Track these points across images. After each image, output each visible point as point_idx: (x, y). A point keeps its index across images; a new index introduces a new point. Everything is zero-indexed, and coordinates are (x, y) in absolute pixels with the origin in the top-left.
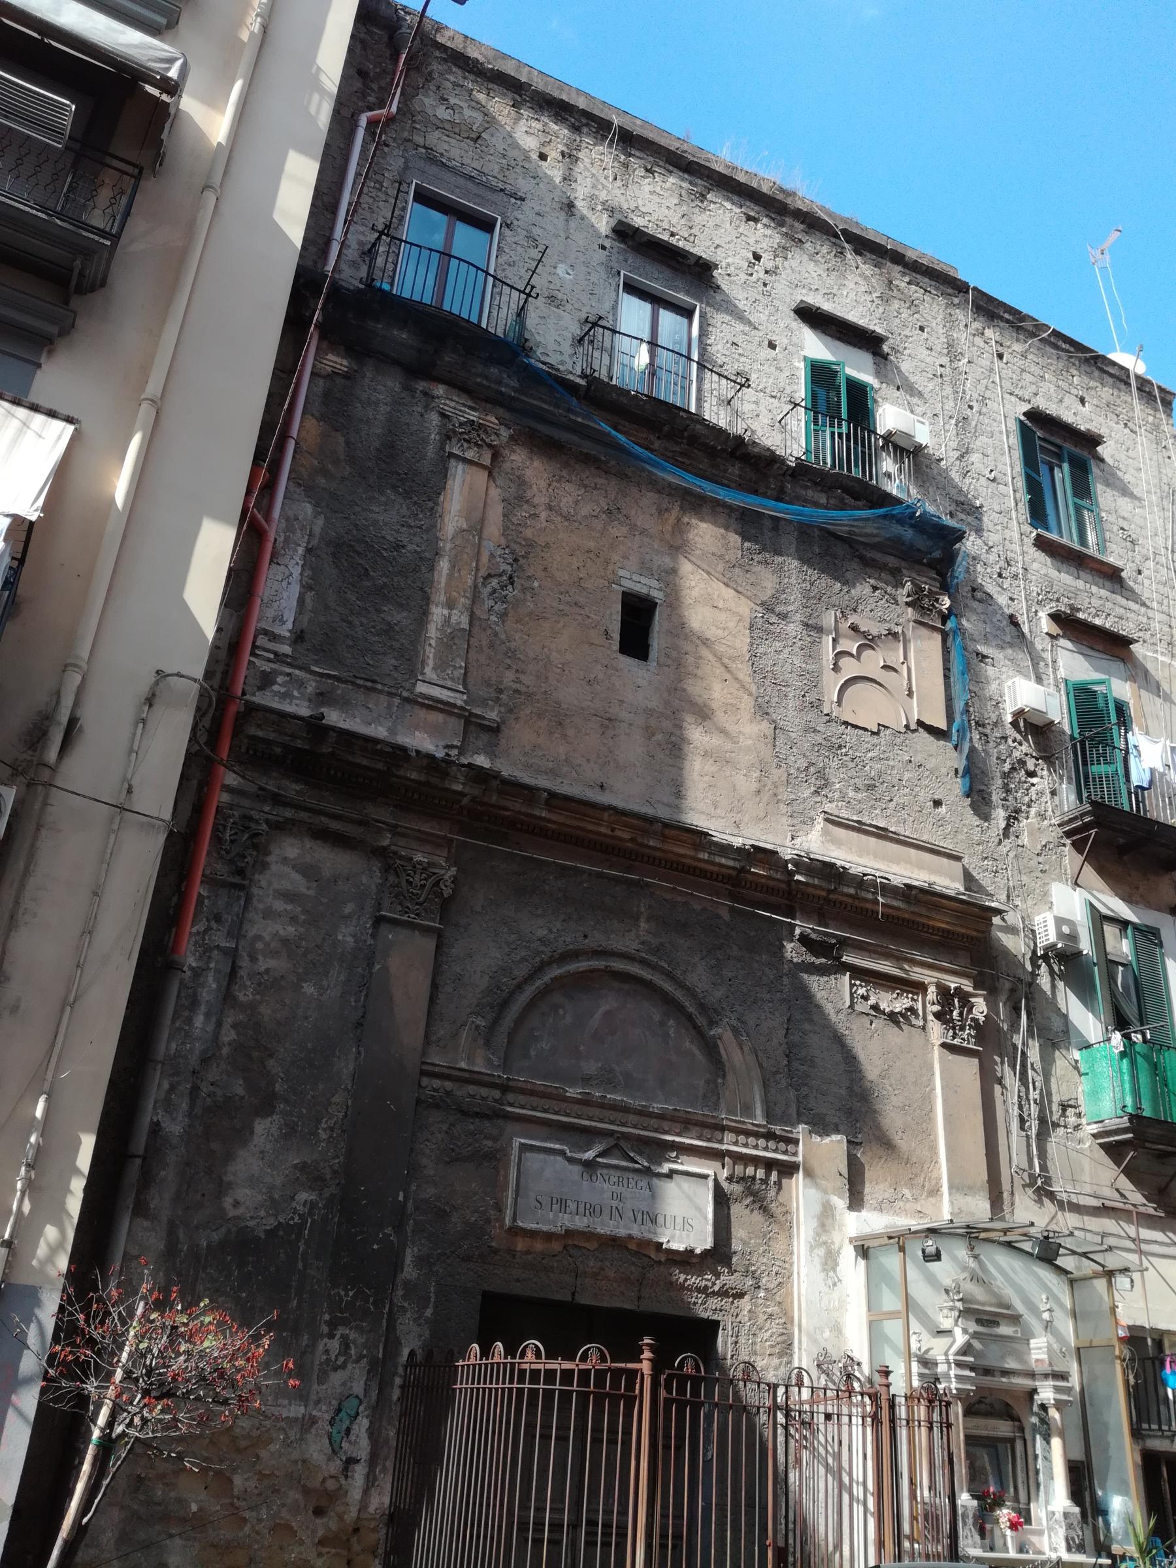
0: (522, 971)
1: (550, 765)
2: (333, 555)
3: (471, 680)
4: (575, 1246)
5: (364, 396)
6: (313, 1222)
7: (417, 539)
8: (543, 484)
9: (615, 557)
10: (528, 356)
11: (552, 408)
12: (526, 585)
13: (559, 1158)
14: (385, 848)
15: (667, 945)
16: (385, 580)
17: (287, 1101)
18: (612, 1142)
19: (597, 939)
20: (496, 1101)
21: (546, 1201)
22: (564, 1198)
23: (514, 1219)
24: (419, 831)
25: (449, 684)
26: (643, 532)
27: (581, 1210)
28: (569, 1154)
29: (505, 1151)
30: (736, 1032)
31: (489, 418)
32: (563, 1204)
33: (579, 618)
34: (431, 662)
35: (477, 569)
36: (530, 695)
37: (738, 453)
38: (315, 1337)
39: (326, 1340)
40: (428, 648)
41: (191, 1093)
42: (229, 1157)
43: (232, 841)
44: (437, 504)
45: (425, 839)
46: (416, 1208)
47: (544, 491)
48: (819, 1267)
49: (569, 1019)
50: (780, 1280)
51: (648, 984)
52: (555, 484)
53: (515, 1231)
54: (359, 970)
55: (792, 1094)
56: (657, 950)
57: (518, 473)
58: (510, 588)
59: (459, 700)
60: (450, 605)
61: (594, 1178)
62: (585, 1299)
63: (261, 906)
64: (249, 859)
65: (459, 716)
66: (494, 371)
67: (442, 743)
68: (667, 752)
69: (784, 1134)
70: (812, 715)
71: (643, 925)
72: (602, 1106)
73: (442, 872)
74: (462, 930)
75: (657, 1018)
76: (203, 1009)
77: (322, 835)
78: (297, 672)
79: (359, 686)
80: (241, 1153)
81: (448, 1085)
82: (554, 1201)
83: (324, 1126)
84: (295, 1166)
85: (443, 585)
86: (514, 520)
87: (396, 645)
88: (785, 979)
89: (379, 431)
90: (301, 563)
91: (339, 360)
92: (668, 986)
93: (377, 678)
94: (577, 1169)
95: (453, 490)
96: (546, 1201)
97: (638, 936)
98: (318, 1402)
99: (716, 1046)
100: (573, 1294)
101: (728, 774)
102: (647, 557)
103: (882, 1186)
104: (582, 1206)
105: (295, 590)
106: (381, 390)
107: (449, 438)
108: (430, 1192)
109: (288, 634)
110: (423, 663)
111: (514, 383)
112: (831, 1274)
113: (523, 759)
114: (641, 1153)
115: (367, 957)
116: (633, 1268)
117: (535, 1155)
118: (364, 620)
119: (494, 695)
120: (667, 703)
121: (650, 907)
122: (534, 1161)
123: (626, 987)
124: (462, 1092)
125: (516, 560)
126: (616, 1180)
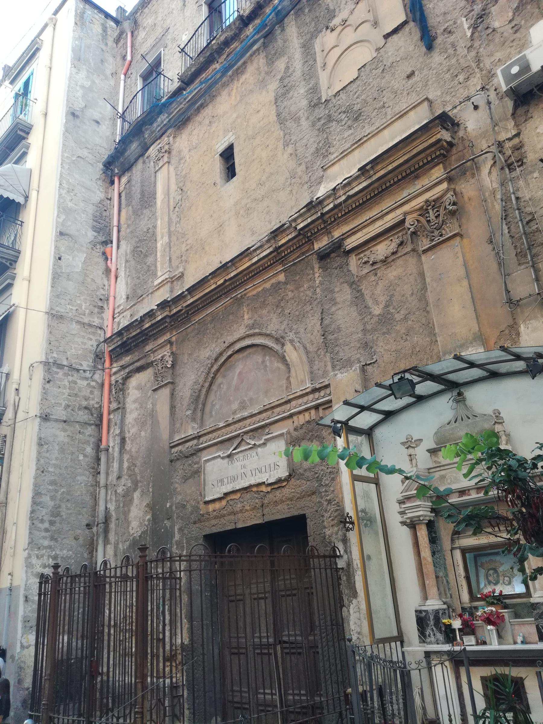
13: (219, 460)
21: (215, 483)
50: (332, 476)
53: (207, 503)
56: (252, 327)
62: (240, 525)
69: (320, 386)
71: (246, 317)
72: (235, 423)
88: (318, 290)
96: (215, 483)
116: (257, 501)
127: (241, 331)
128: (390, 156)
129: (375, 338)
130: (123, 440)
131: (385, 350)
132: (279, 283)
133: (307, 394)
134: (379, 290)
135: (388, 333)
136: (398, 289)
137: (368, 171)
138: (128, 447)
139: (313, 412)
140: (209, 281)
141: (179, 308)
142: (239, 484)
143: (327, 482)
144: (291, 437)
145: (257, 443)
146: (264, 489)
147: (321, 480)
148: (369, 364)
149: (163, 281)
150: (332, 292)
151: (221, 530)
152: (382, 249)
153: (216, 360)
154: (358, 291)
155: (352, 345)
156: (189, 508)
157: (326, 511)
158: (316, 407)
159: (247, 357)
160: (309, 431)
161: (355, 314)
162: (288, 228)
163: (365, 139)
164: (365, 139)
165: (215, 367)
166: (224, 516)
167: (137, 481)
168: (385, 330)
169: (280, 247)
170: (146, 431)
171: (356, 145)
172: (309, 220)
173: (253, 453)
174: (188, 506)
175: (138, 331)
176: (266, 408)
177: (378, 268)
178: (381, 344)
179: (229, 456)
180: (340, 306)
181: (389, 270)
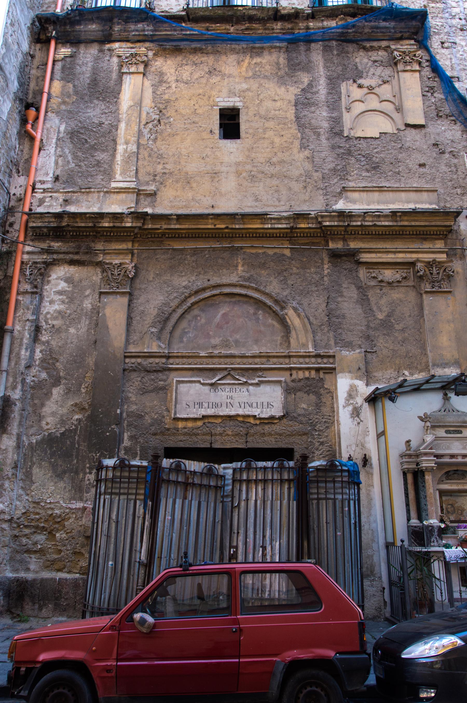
0: (176, 302)
1: (184, 204)
2: (70, 138)
3: (140, 175)
4: (209, 422)
5: (80, 62)
6: (81, 427)
7: (110, 118)
8: (173, 71)
9: (214, 93)
10: (153, 12)
11: (173, 33)
12: (166, 121)
13: (198, 385)
14: (100, 262)
15: (255, 275)
16: (95, 141)
17: (65, 379)
18: (226, 373)
19: (215, 280)
20: (163, 364)
21: (191, 404)
22: (201, 401)
23: (175, 414)
24: (115, 250)
25: (128, 179)
26: (230, 76)
27: (211, 406)
28: (202, 381)
29: (170, 385)
30: (295, 309)
31: (141, 49)
32: (200, 405)
33: (196, 129)
34: (119, 172)
35: (140, 122)
36: (171, 173)
37: (278, 16)
38: (85, 473)
39: (88, 475)
40: (117, 166)
41: (22, 382)
42: (43, 405)
43: (31, 274)
44: (118, 99)
45: (119, 252)
46: (128, 416)
47: (174, 74)
48: (349, 416)
49: (203, 321)
51: (246, 296)
52: (179, 69)
54: (95, 318)
55: (331, 334)
56: (248, 279)
57: (159, 70)
58: (159, 126)
59: (133, 185)
60: (127, 143)
61: (217, 391)
62: (216, 446)
63: (48, 299)
64: (38, 280)
65: (133, 192)
66: (140, 26)
67: (126, 207)
68: (249, 181)
69: (325, 354)
70: (337, 139)
71: (240, 268)
72: (220, 357)
73: (127, 266)
74: (143, 290)
75: (252, 311)
76: (24, 347)
77: (72, 263)
78: (54, 194)
79: (83, 193)
80: (47, 403)
81: (139, 360)
82: (196, 403)
83: (83, 386)
84: (72, 405)
85: (123, 134)
86: (159, 93)
87: (102, 169)
88: (326, 279)
89: (88, 76)
90: (54, 146)
91: (66, 50)
92: (256, 295)
93: (90, 186)
94: (207, 388)
95: (125, 90)
96: (191, 404)
97: (238, 274)
98: (87, 500)
99: (285, 318)
100: (211, 443)
101: (286, 182)
102: (232, 88)
103: (389, 372)
104: (211, 404)
105: (53, 159)
106: (88, 55)
107: (122, 66)
108: (134, 408)
109: (50, 179)
110: (115, 174)
111: (151, 28)
112: (357, 418)
113: (169, 204)
114: (243, 376)
115: (96, 311)
116: (242, 429)
117: (185, 385)
118: (86, 163)
119: (152, 178)
120: (248, 157)
121: (244, 259)
122: (183, 388)
123: (233, 300)
124: (146, 362)
125: (161, 111)
126: (229, 390)
127: (234, 279)
128: (416, 216)
129: (377, 335)
130: (37, 329)
131: (384, 346)
132: (284, 255)
133: (309, 357)
134: (383, 301)
135: (388, 335)
136: (399, 308)
137: (396, 216)
138: (44, 338)
139: (313, 372)
140: (207, 219)
141: (158, 226)
142: (222, 411)
143: (321, 428)
144: (287, 385)
145: (249, 381)
146: (252, 420)
147: (315, 426)
148: (369, 352)
149: (129, 188)
150: (340, 285)
151: (191, 446)
152: (388, 274)
153: (197, 292)
154: (365, 295)
155: (355, 333)
156: (148, 420)
157: (317, 449)
158: (318, 370)
159: (235, 303)
160: (308, 386)
161: (360, 311)
162: (312, 218)
163: (386, 189)
164: (386, 189)
165: (193, 299)
166: (198, 434)
167: (60, 377)
168: (385, 332)
169: (296, 228)
170: (78, 330)
171: (377, 189)
172: (336, 223)
173: (244, 389)
174: (147, 417)
175: (90, 225)
176: (262, 354)
177: (384, 286)
178: (381, 341)
179: (212, 385)
180: (346, 299)
181: (392, 291)
